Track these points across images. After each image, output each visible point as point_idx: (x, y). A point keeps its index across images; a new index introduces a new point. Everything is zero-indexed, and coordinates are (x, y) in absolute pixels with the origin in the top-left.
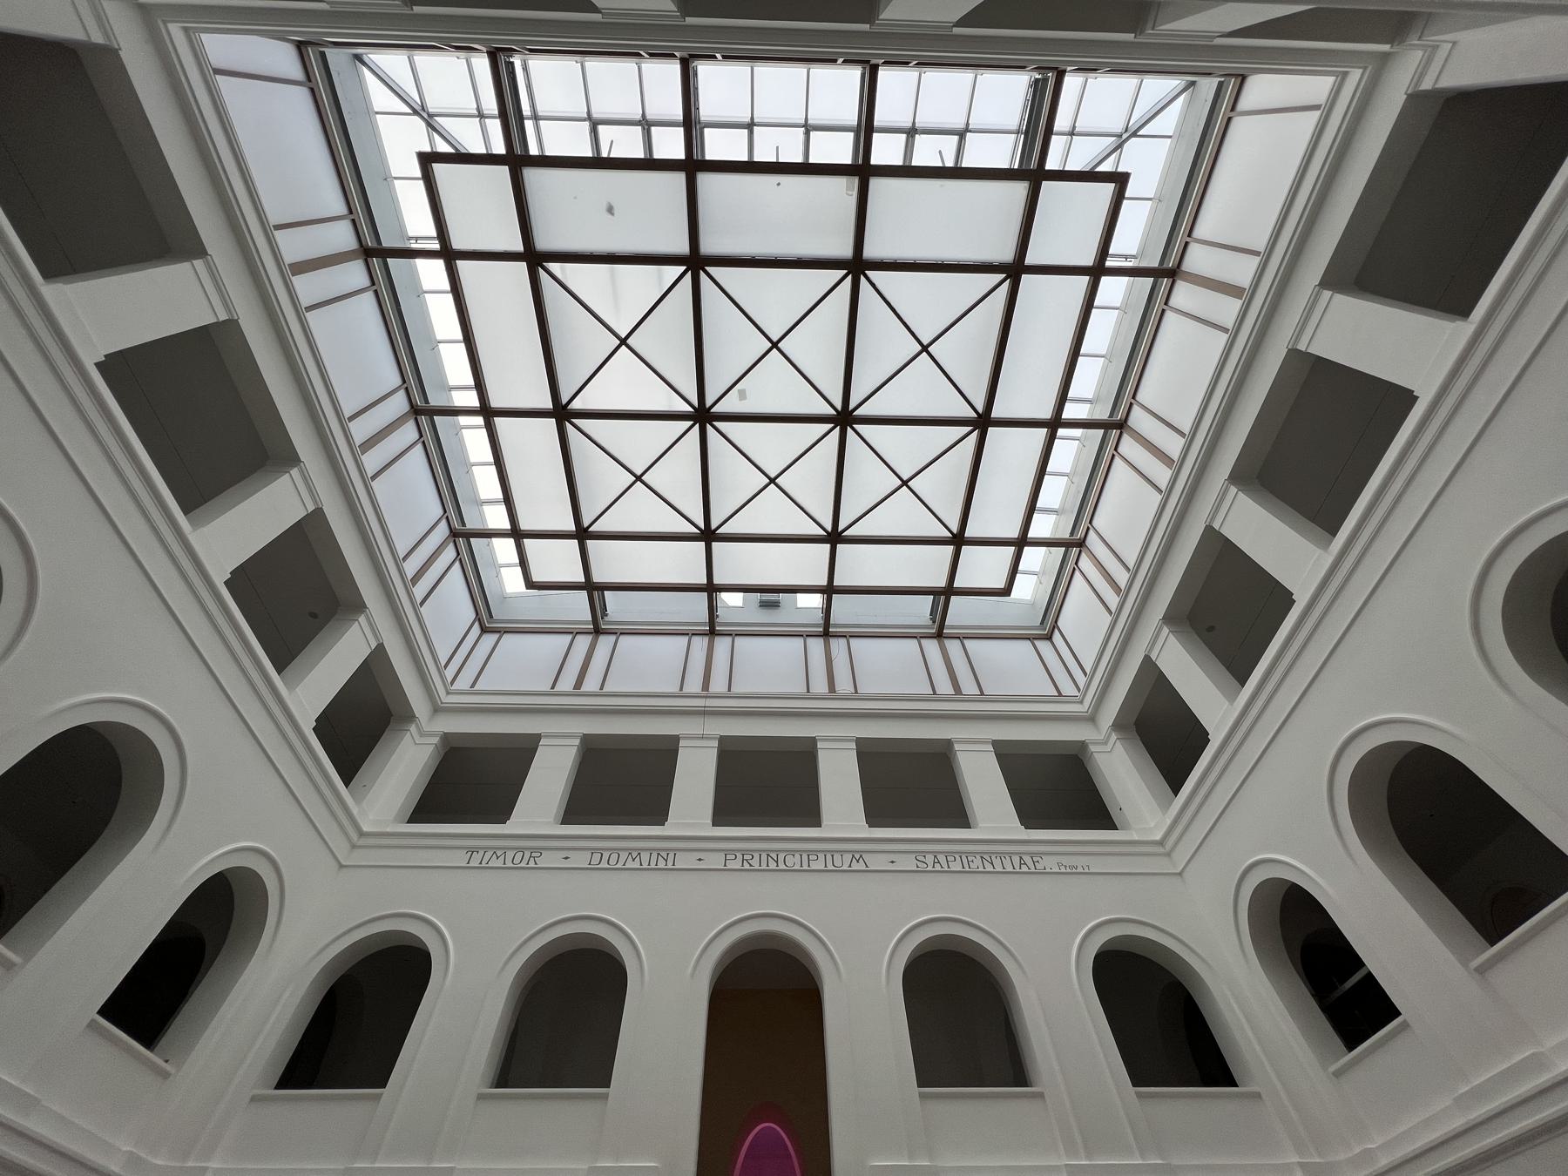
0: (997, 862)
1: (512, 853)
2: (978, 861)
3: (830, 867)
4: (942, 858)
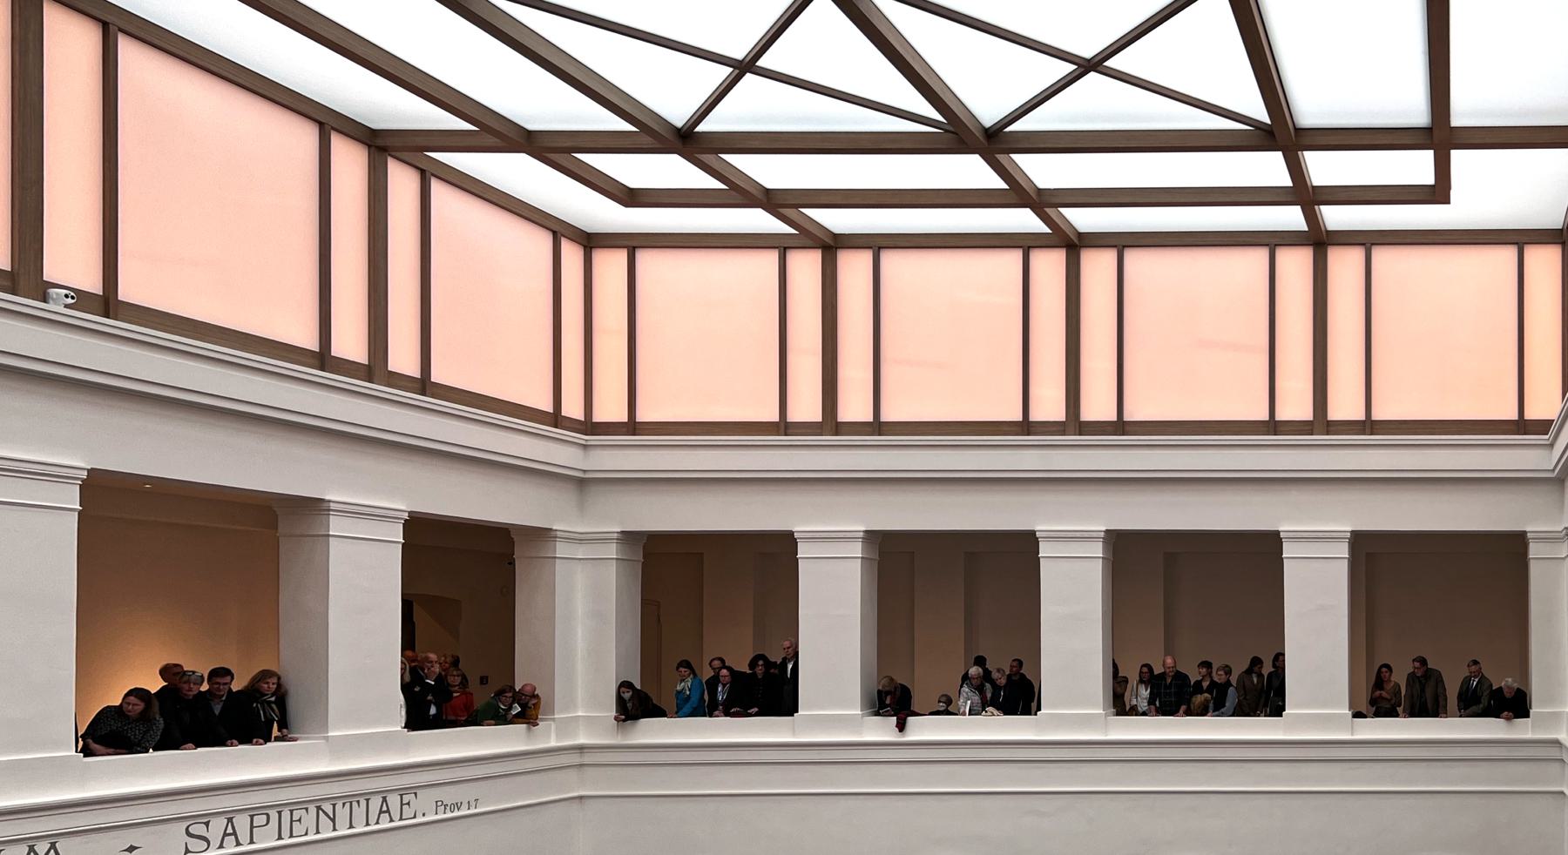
0: (342, 813)
2: (309, 819)
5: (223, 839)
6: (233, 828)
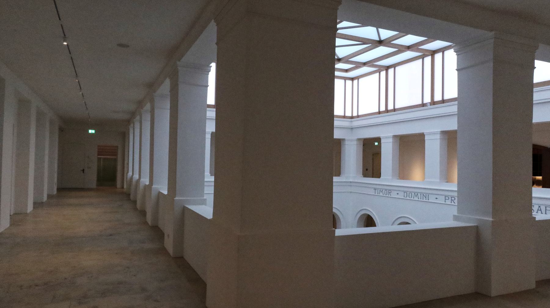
1: (385, 190)
5: (537, 211)
6: (541, 209)
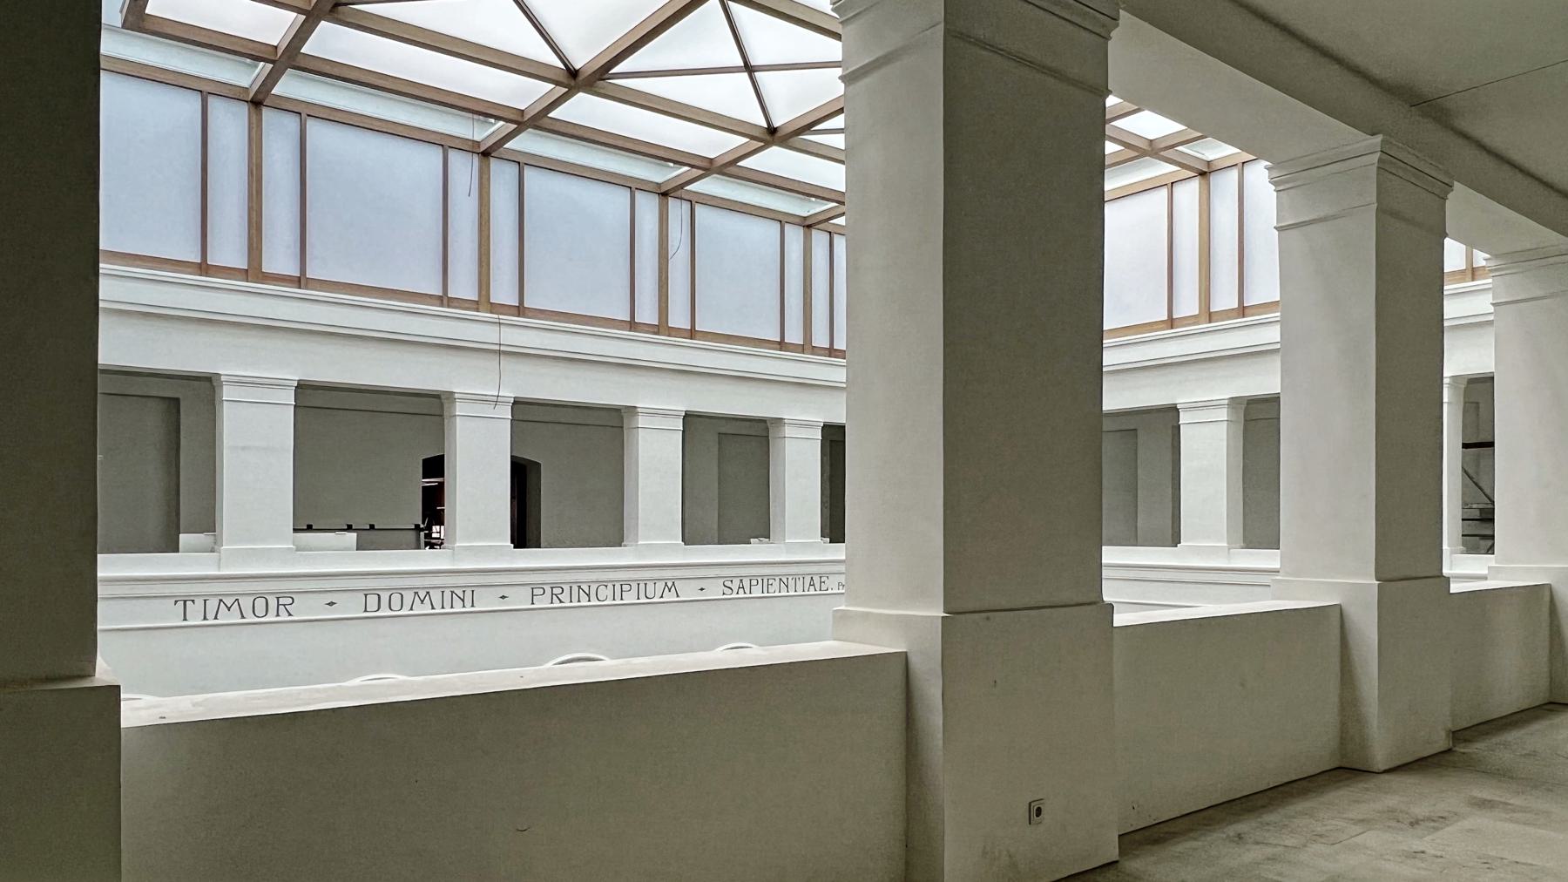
0: (791, 583)
3: (644, 600)
4: (746, 583)
